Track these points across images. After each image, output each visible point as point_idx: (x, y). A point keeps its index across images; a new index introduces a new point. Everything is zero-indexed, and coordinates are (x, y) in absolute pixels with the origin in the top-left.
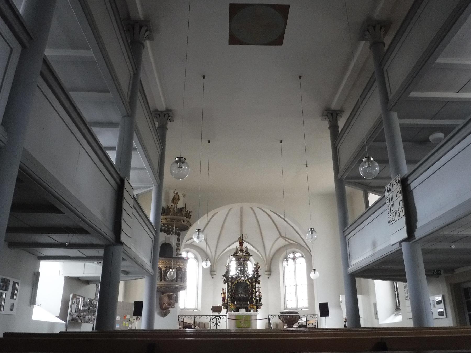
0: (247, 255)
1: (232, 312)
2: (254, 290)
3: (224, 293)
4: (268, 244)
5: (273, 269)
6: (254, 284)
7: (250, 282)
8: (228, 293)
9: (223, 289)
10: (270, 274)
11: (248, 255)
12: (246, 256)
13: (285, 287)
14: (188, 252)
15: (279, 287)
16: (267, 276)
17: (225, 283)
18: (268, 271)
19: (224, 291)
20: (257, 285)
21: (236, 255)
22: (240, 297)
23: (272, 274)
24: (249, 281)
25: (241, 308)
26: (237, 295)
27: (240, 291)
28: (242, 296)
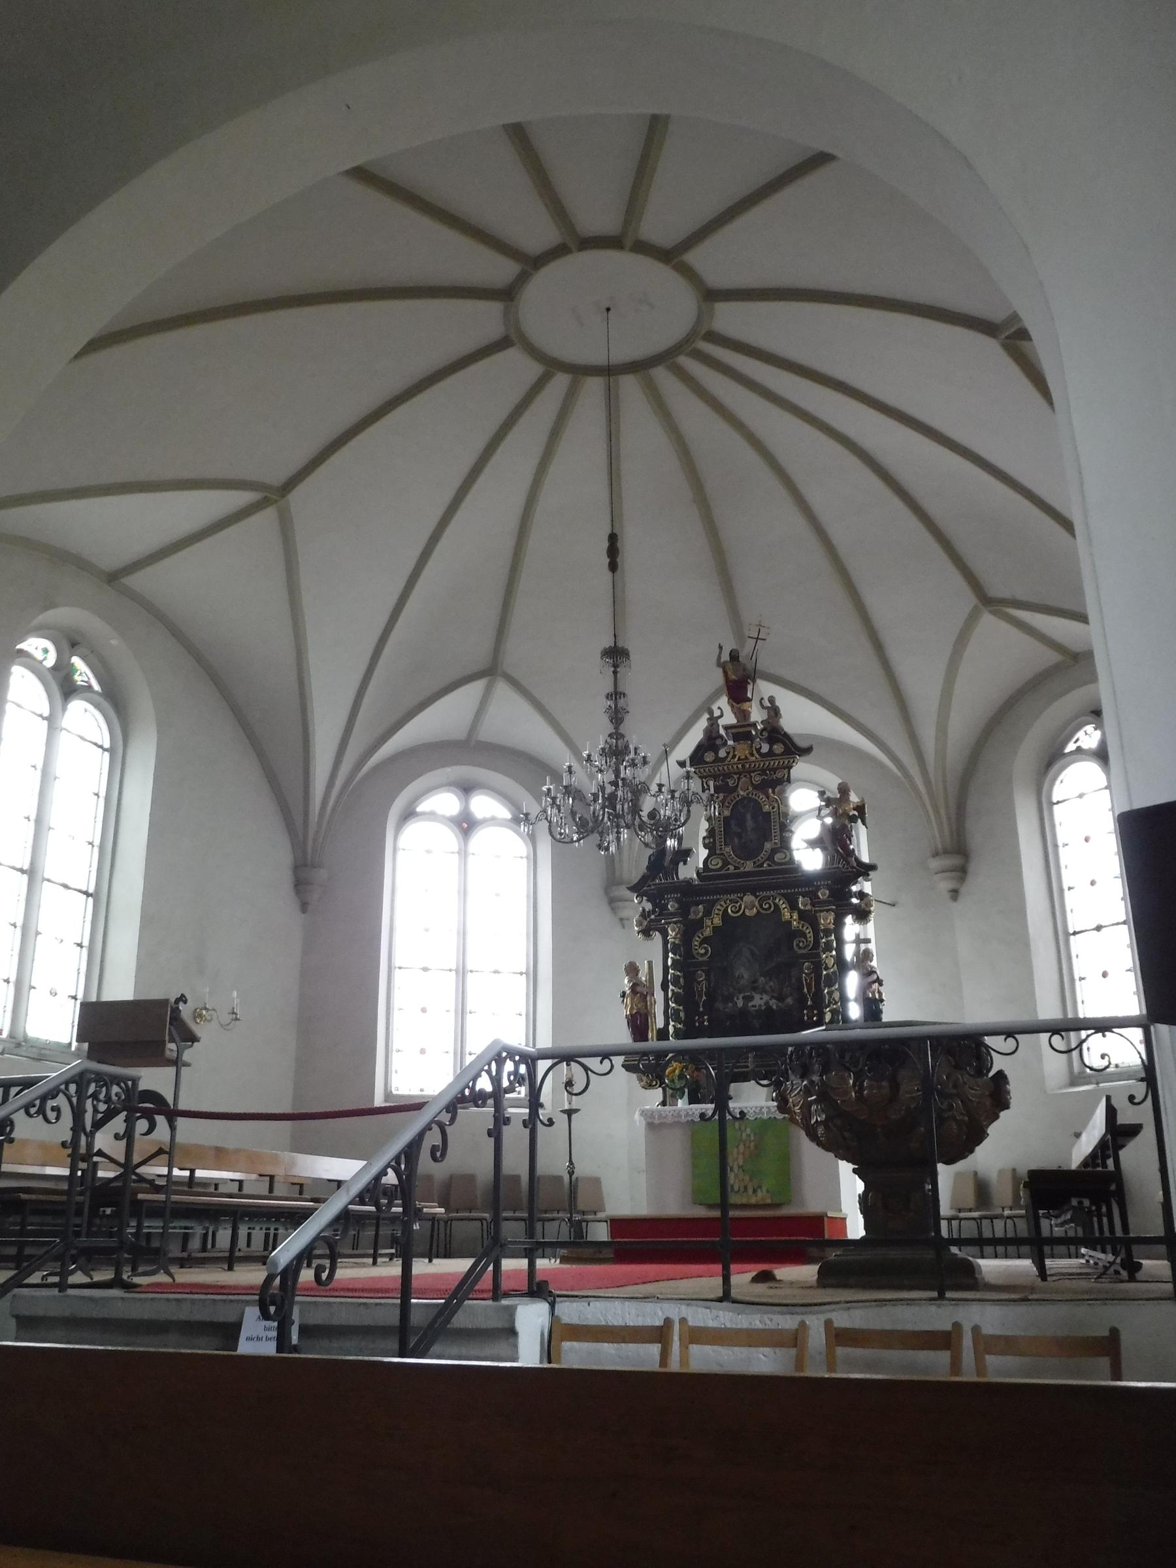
0: (778, 748)
1: (682, 1104)
2: (829, 958)
3: (639, 992)
4: (922, 681)
5: (976, 837)
6: (826, 920)
7: (803, 916)
8: (664, 987)
9: (632, 970)
10: (961, 872)
11: (783, 749)
12: (771, 753)
13: (1062, 936)
14: (466, 789)
15: (1021, 942)
16: (944, 885)
17: (646, 933)
18: (946, 852)
19: (643, 976)
20: (851, 928)
21: (709, 757)
22: (744, 1012)
23: (972, 867)
24: (793, 906)
25: (744, 1078)
26: (730, 998)
27: (744, 973)
28: (758, 1001)
